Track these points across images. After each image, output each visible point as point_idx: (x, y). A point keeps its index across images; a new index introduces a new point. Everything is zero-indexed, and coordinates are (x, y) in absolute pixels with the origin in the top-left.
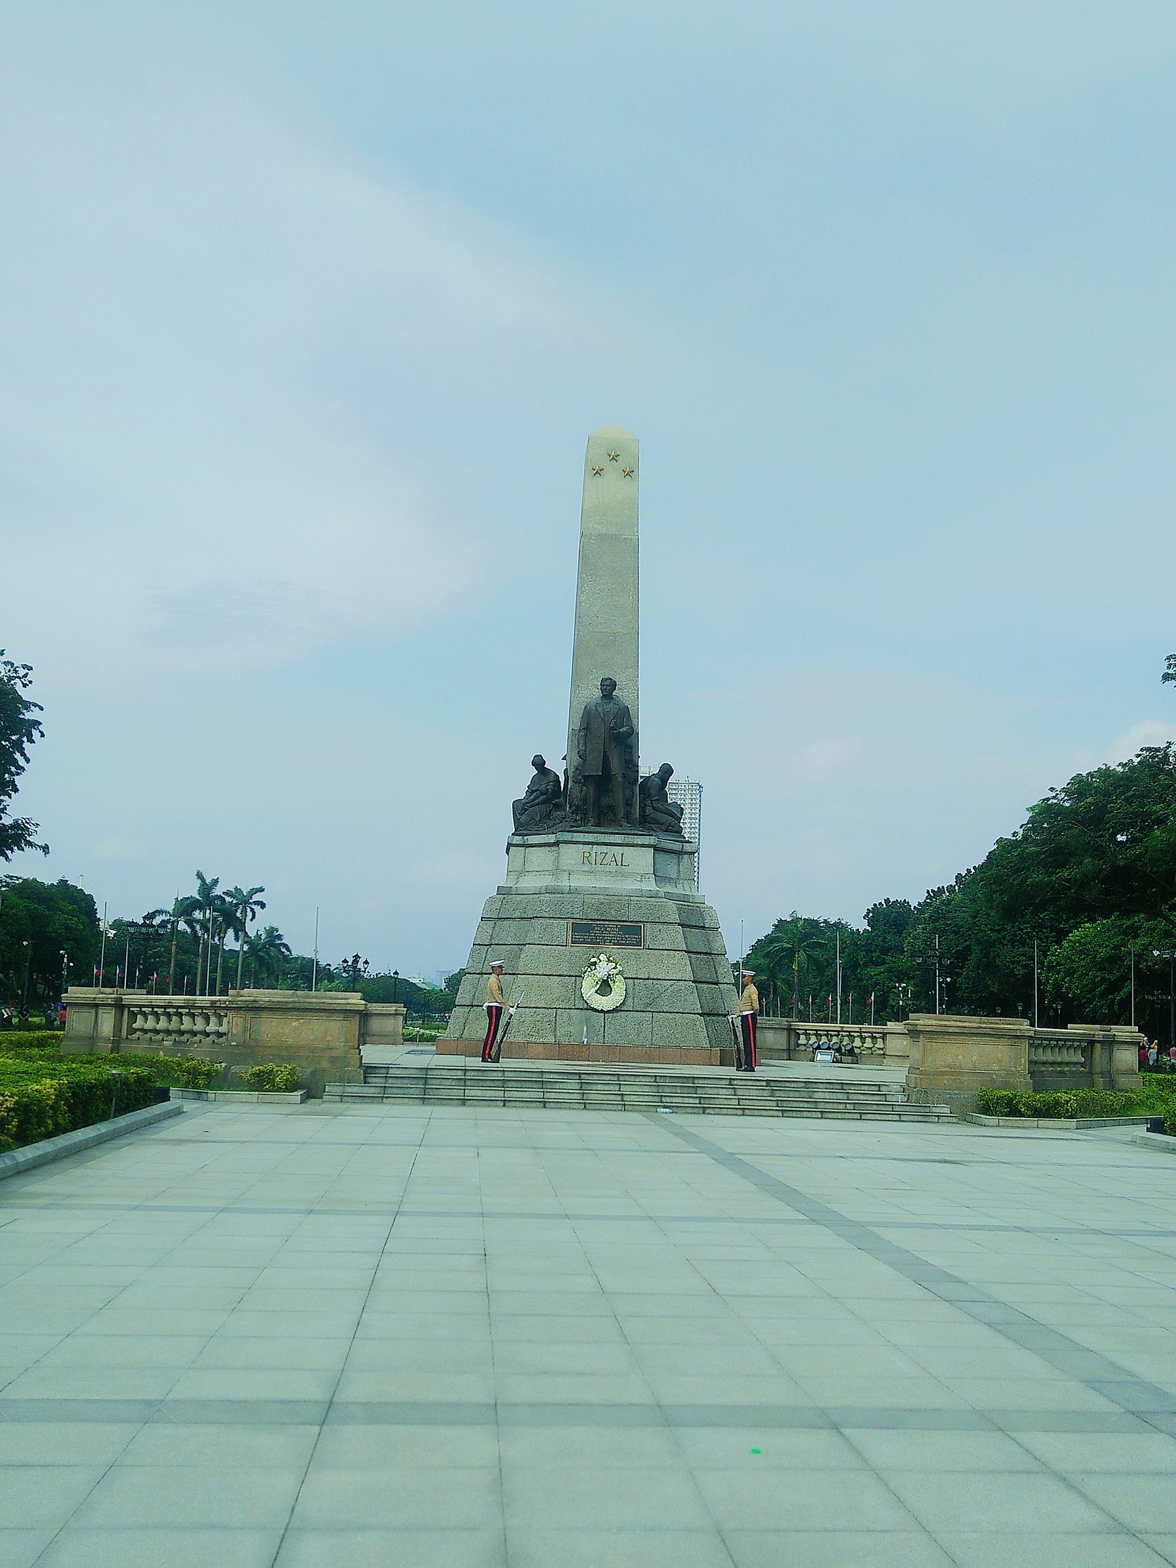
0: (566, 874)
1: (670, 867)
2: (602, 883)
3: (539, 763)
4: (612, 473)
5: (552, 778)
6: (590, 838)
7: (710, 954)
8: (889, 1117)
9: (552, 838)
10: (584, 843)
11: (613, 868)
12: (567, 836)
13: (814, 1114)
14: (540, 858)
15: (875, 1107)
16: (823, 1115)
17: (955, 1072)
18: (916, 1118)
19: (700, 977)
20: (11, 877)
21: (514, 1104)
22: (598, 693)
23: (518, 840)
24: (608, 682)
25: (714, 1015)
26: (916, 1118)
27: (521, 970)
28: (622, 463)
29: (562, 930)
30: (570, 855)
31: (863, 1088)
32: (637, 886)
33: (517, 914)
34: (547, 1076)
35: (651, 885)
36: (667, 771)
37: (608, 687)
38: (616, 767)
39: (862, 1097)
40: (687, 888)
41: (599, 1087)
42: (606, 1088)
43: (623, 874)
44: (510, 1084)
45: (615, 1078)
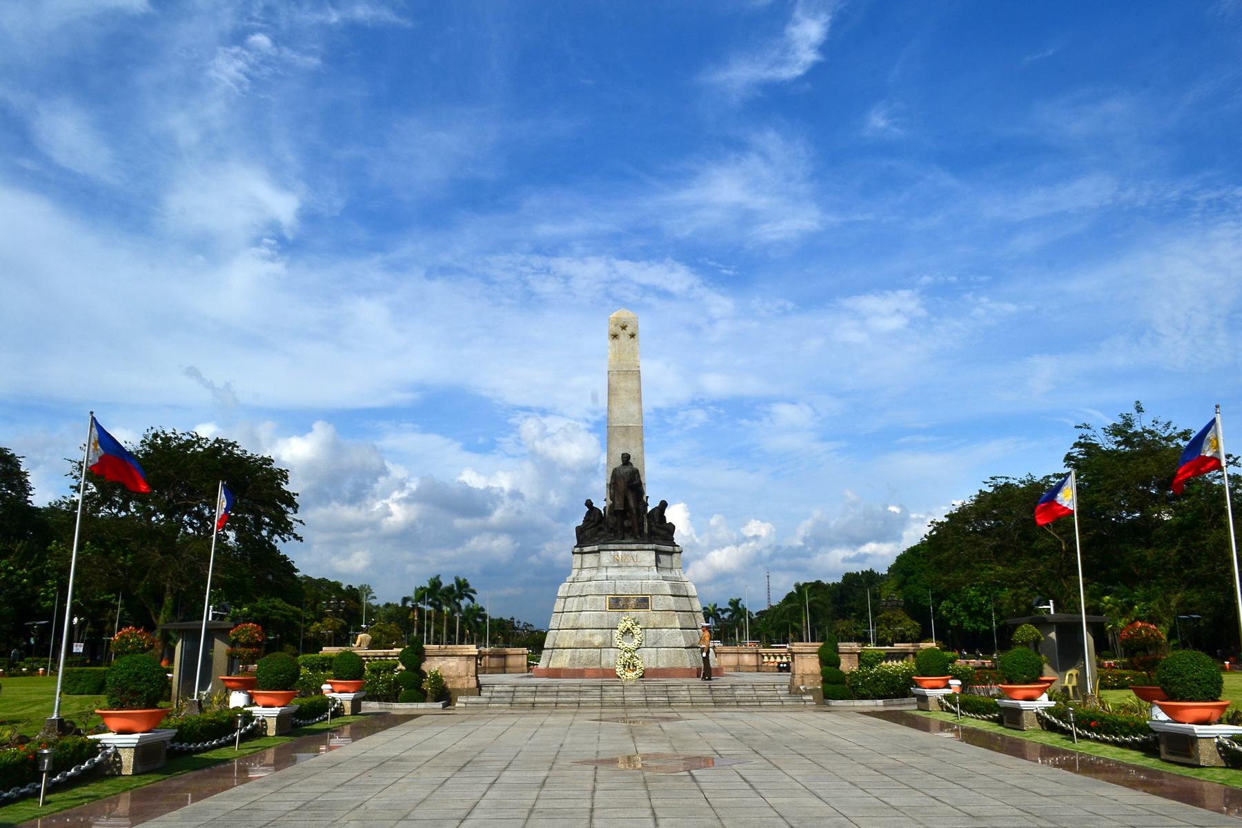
3: (589, 504)
4: (624, 337)
6: (617, 546)
9: (596, 548)
12: (605, 547)
14: (590, 560)
16: (738, 704)
19: (685, 625)
23: (577, 550)
28: (629, 330)
29: (604, 602)
30: (606, 557)
32: (646, 573)
36: (664, 505)
37: (626, 459)
38: (632, 503)
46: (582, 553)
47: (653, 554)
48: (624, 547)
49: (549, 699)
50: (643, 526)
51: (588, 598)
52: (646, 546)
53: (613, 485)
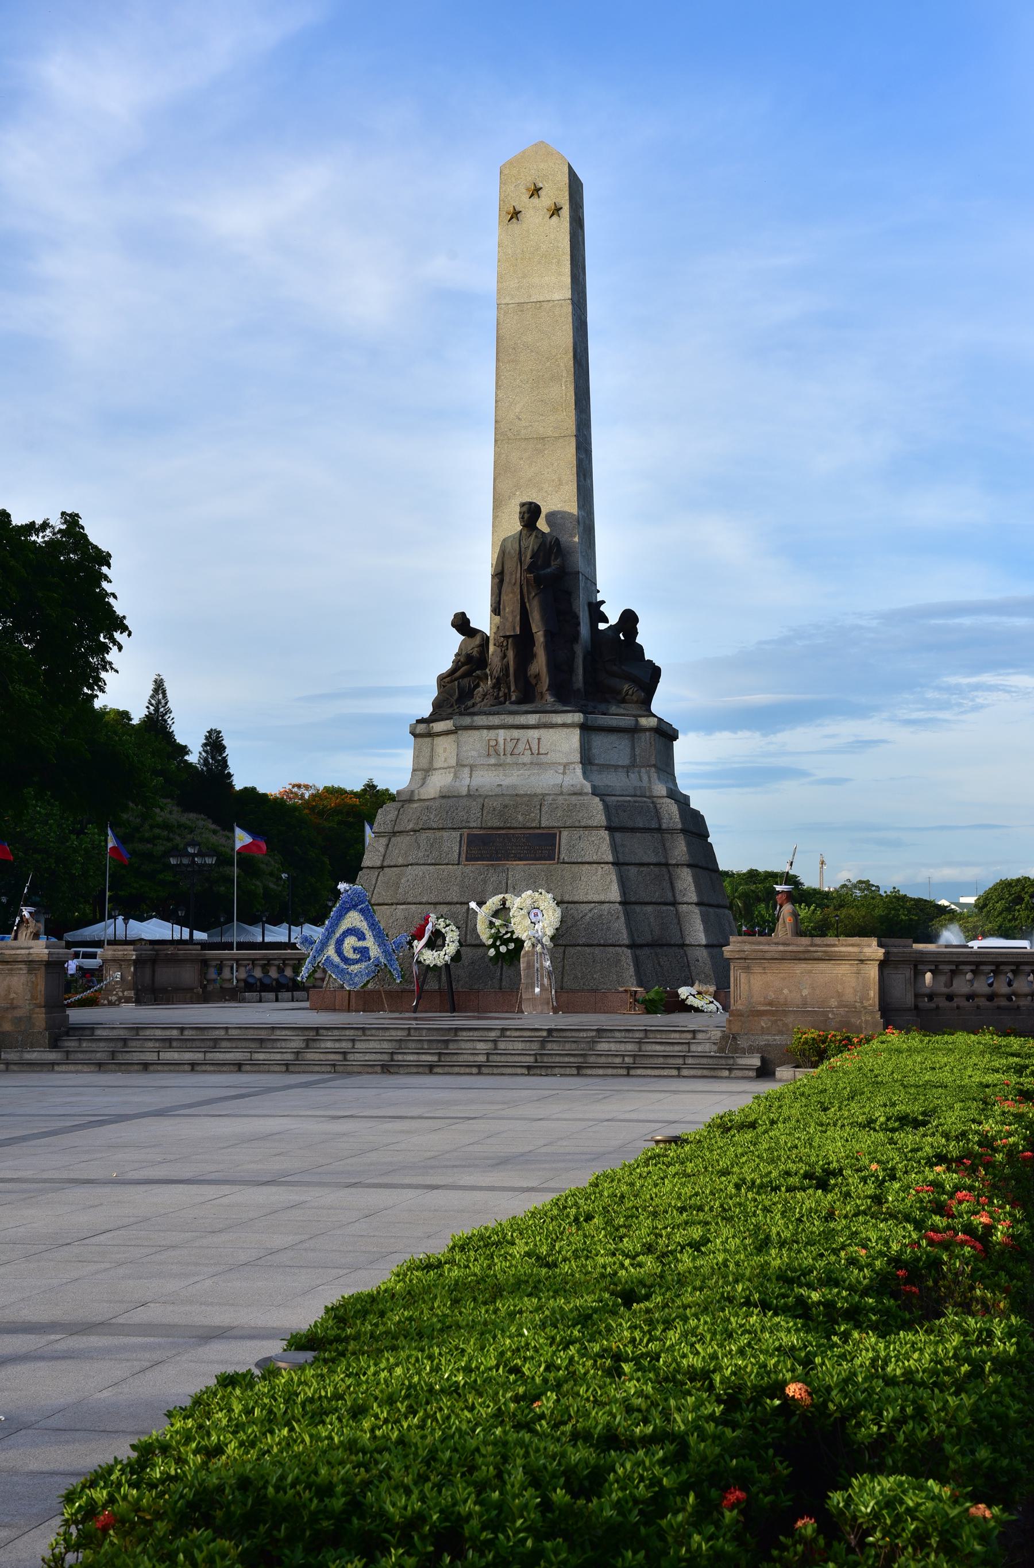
0: (467, 770)
1: (612, 749)
2: (513, 780)
3: (461, 623)
5: (477, 640)
7: (667, 865)
8: (665, 1072)
10: (489, 728)
11: (527, 758)
12: (467, 721)
13: (568, 1071)
14: (445, 749)
15: (661, 1060)
17: (776, 1011)
18: (699, 1073)
20: (299, 786)
21: (204, 1068)
22: (517, 527)
23: (421, 728)
24: (525, 509)
25: (662, 945)
26: (699, 1073)
27: (400, 897)
29: (452, 843)
30: (474, 743)
31: (673, 1035)
32: (558, 779)
33: (411, 826)
34: (278, 1032)
35: (576, 777)
36: (629, 619)
39: (658, 1047)
40: (645, 778)
41: (329, 1044)
42: (337, 1045)
43: (539, 765)
44: (224, 1044)
45: (360, 1033)
46: (430, 735)
47: (577, 731)
48: (510, 720)
49: (188, 1056)
50: (571, 670)
51: (423, 836)
52: (559, 719)
53: (499, 577)
